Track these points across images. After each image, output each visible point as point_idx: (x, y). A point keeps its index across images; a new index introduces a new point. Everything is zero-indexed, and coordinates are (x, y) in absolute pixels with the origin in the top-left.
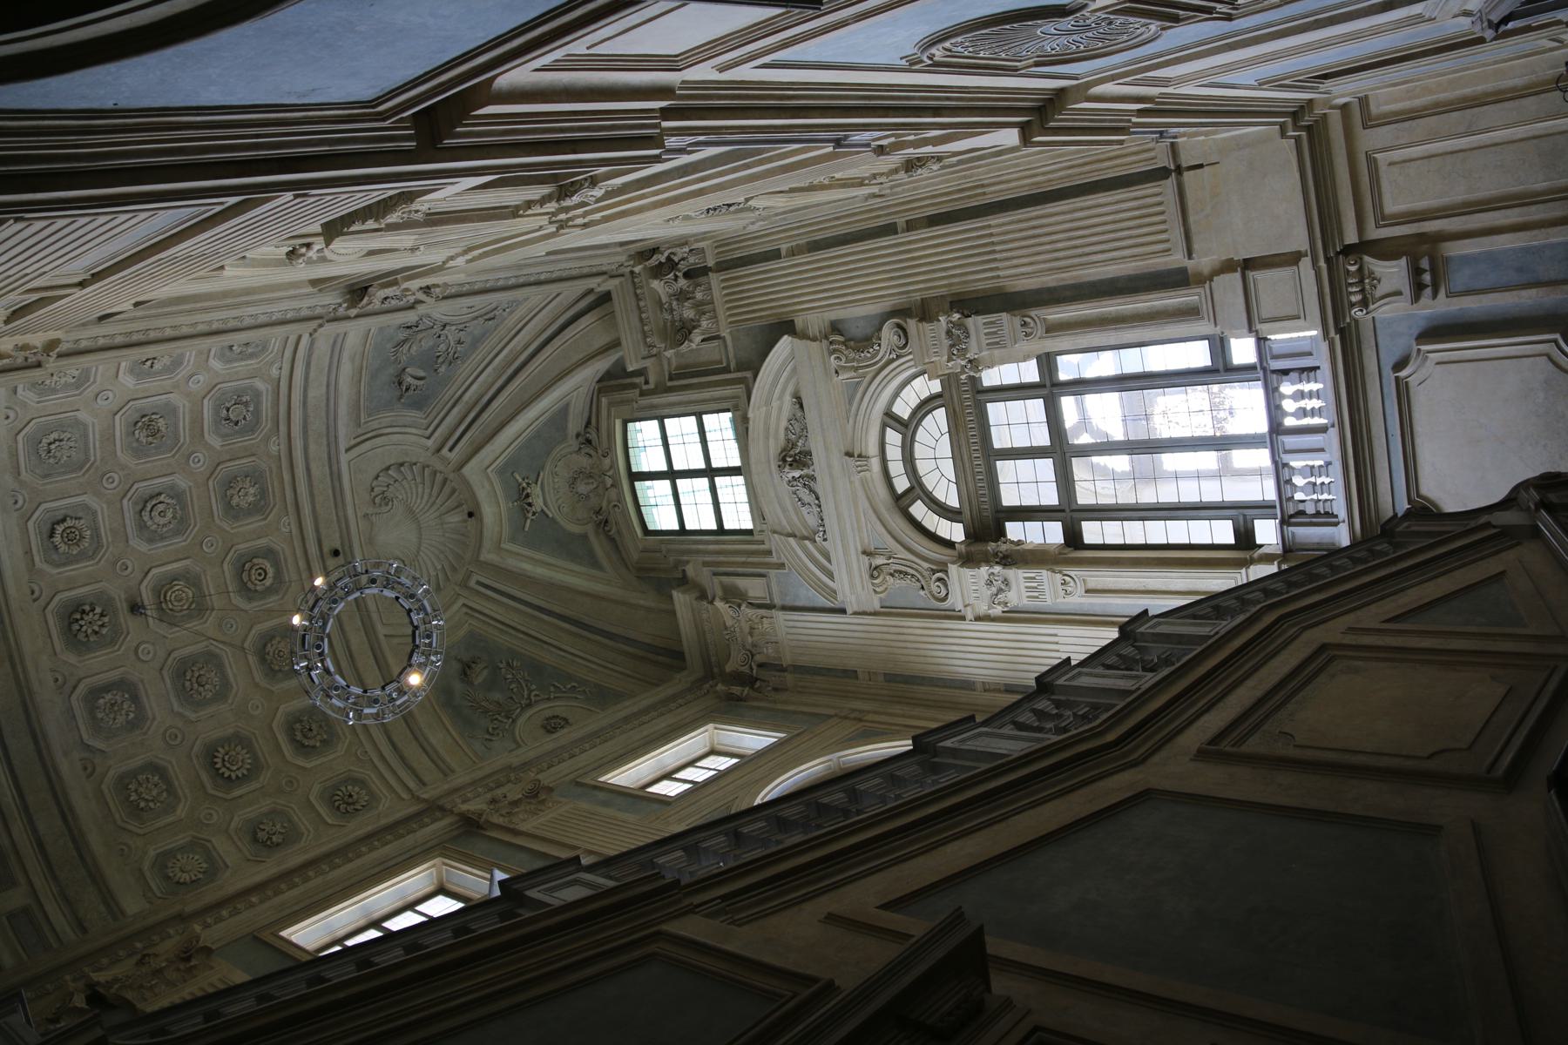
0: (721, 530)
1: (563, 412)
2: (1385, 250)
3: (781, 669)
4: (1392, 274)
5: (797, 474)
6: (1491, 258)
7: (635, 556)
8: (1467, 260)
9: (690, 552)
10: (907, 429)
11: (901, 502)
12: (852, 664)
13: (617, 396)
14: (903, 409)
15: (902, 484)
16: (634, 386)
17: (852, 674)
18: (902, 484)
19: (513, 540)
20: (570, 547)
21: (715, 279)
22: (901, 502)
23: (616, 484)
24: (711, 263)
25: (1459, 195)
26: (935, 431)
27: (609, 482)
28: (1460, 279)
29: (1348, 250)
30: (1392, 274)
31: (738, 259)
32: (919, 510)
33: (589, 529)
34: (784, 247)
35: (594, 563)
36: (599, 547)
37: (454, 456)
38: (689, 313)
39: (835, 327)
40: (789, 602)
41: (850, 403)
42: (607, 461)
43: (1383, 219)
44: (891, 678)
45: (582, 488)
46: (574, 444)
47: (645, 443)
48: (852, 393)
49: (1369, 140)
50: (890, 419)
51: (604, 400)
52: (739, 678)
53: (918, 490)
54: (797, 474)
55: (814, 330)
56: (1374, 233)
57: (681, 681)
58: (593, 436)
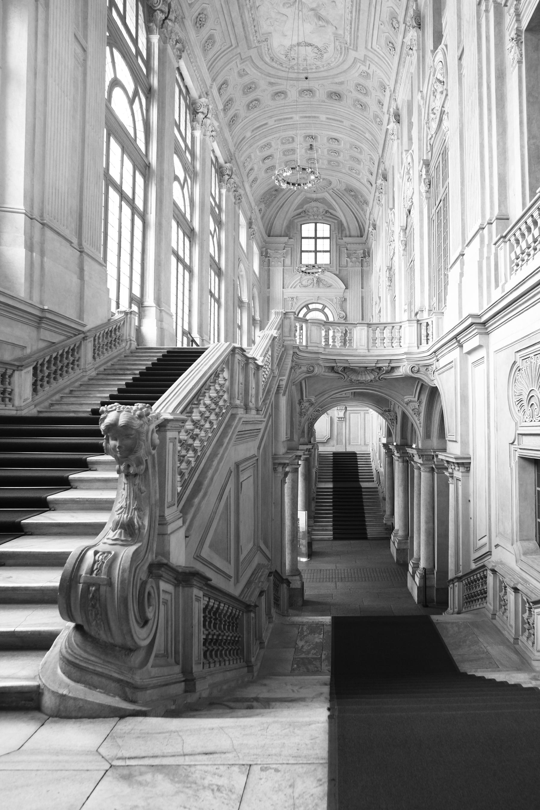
0: (302, 251)
1: (335, 210)
2: (345, 413)
3: (269, 266)
4: (341, 414)
5: (315, 281)
6: (342, 429)
7: (296, 221)
8: (342, 425)
9: (297, 242)
10: (322, 311)
11: (307, 306)
12: (271, 287)
13: (337, 227)
14: (326, 310)
15: (311, 306)
16: (339, 233)
17: (269, 288)
18: (311, 306)
19: (306, 197)
20: (301, 205)
21: (360, 269)
22: (307, 306)
23: (315, 219)
24: (364, 268)
25: (351, 425)
26: (321, 317)
27: (315, 209)
28: (339, 424)
29: (346, 408)
30: (341, 414)
31: (364, 276)
32: (305, 310)
33: (304, 209)
34: (364, 290)
35: (295, 210)
36: (300, 210)
37: (331, 192)
38: (354, 259)
39: (345, 300)
40: (285, 271)
41: (329, 300)
42: (321, 218)
43: (350, 414)
44: (268, 298)
45: (315, 209)
46: (327, 209)
47: (324, 230)
48: (332, 300)
49: (362, 413)
50: (324, 307)
51: (336, 221)
52: (267, 253)
53: (309, 310)
54: (315, 281)
55: (345, 294)
56: (348, 412)
57: (265, 236)
58: (328, 215)
